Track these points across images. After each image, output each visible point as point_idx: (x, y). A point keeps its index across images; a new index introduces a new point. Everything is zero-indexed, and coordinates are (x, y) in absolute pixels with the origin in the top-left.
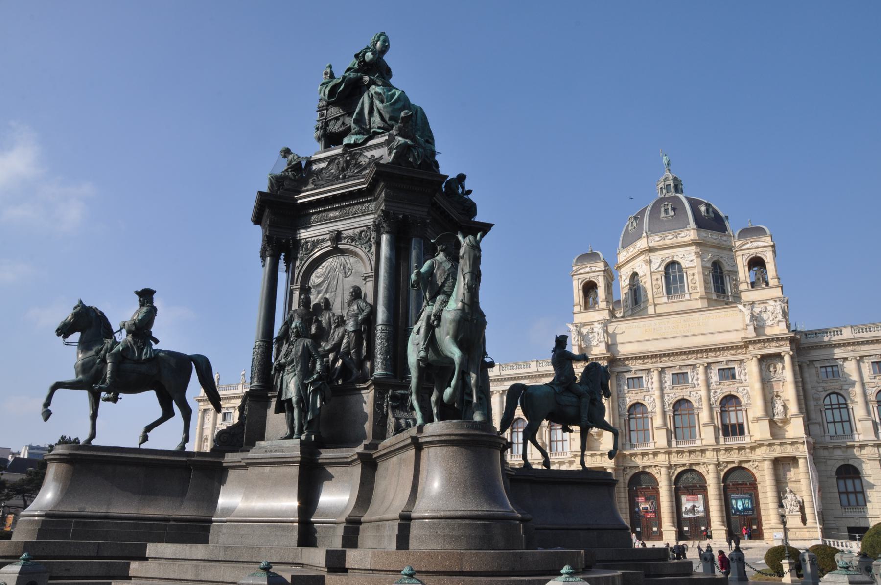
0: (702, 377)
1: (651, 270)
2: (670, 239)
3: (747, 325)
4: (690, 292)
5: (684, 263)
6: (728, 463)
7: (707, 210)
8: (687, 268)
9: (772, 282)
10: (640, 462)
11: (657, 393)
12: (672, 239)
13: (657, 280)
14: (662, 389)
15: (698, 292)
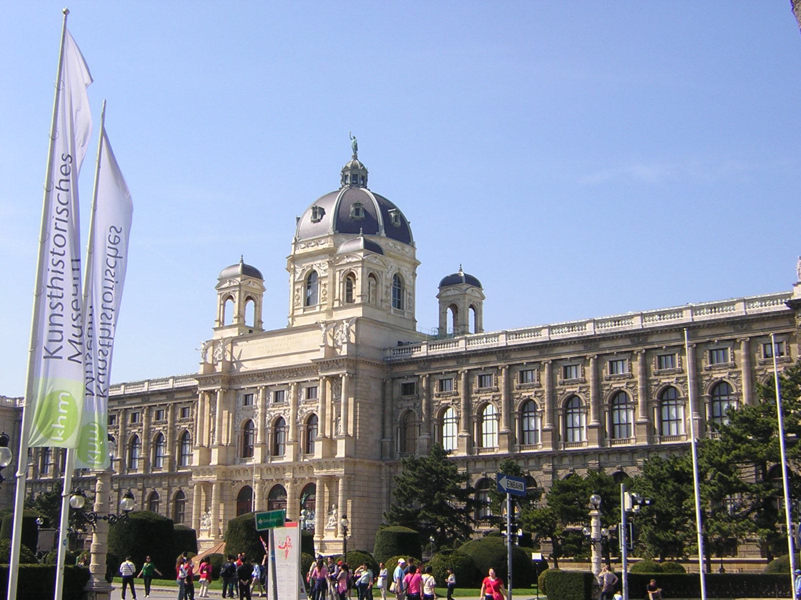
0: (292, 395)
1: (294, 280)
2: (312, 246)
3: (321, 346)
4: (321, 303)
5: (320, 273)
6: (303, 479)
7: (357, 211)
8: (321, 278)
9: (358, 300)
10: (242, 478)
11: (259, 410)
12: (312, 246)
13: (298, 290)
14: (265, 407)
15: (326, 304)
